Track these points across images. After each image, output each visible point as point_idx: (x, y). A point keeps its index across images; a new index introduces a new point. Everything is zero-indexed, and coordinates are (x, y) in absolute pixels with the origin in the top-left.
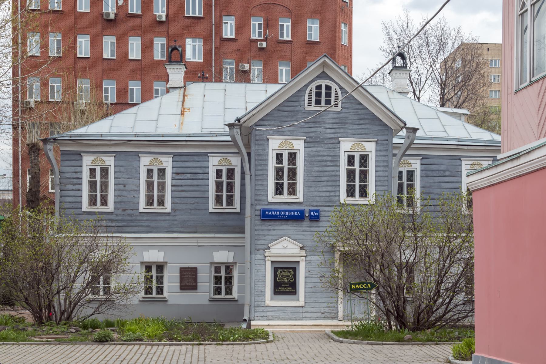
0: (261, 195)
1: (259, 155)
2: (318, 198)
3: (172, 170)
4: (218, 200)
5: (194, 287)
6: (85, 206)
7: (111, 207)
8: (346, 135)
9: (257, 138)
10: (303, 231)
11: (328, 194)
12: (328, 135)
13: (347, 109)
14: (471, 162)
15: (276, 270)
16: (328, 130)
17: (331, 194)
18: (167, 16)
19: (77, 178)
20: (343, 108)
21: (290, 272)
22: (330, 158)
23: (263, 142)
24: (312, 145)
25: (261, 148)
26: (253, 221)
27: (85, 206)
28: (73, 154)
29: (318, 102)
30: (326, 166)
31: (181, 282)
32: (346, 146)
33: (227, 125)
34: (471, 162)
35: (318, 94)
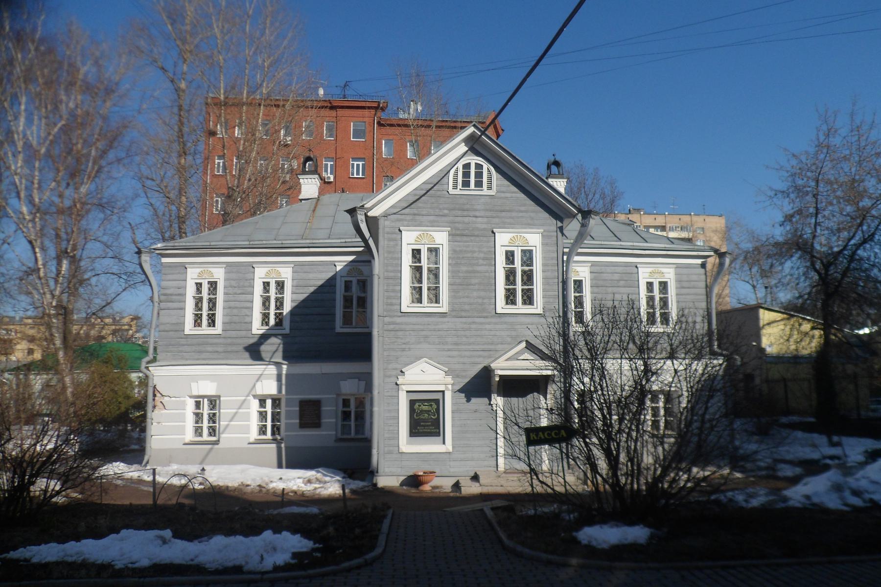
0: (391, 304)
1: (389, 252)
2: (467, 307)
5: (317, 425)
6: (189, 327)
7: (218, 329)
8: (504, 226)
9: (387, 230)
10: (449, 350)
11: (480, 301)
12: (479, 226)
13: (503, 192)
14: (650, 270)
15: (412, 403)
16: (479, 219)
17: (485, 301)
18: (335, 178)
19: (179, 295)
20: (498, 192)
21: (431, 405)
22: (482, 255)
23: (395, 236)
24: (458, 238)
25: (392, 243)
26: (381, 338)
27: (189, 327)
28: (176, 266)
29: (466, 184)
30: (477, 265)
31: (300, 419)
32: (503, 239)
33: (346, 211)
34: (650, 270)
35: (466, 174)
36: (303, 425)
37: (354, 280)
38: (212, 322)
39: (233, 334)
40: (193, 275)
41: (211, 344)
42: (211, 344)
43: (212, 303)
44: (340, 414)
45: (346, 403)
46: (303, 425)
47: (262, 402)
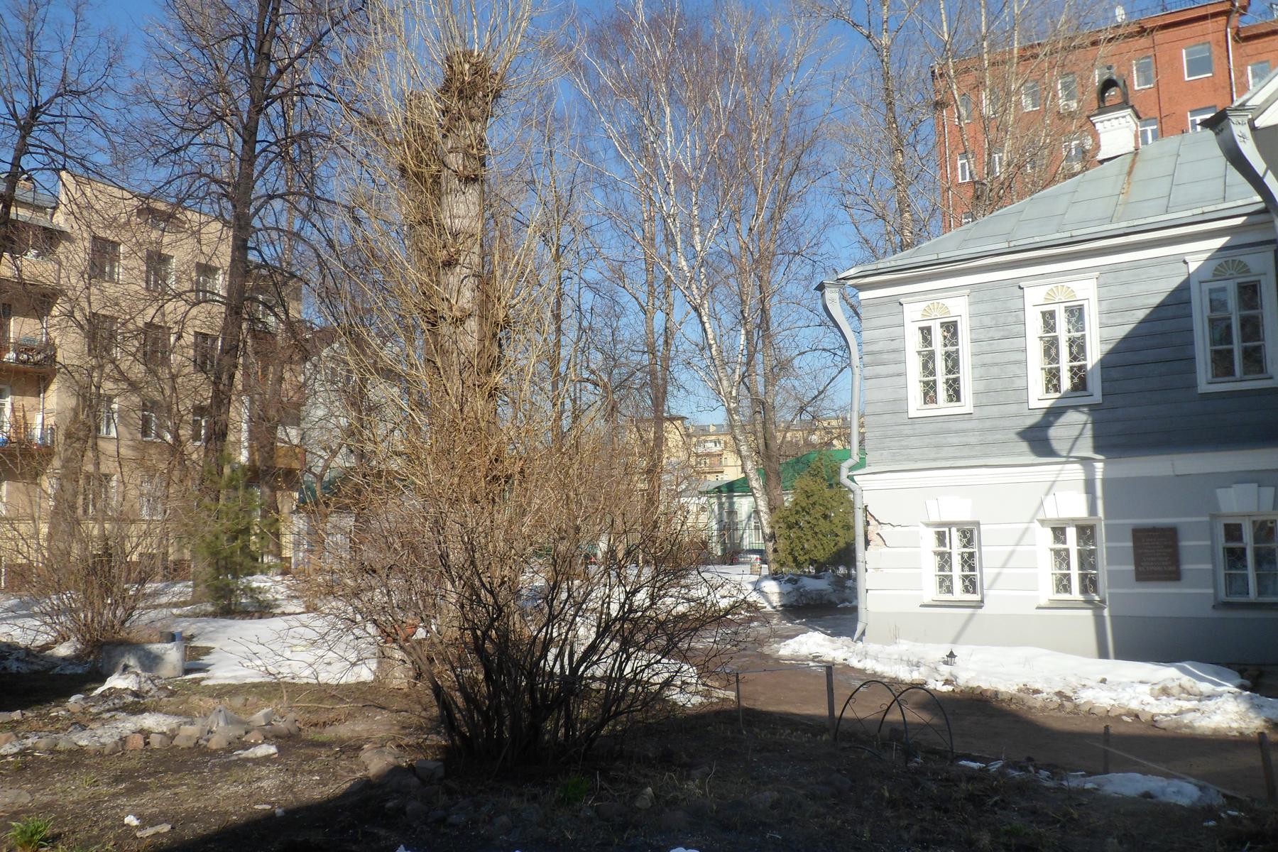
3: (1100, 305)
4: (1222, 363)
5: (1173, 574)
6: (915, 405)
27: (915, 405)
28: (884, 303)
36: (1143, 575)
37: (1231, 286)
38: (955, 393)
39: (994, 411)
40: (914, 314)
41: (956, 432)
42: (956, 432)
43: (953, 362)
44: (1220, 554)
45: (1233, 532)
46: (1143, 575)
47: (1059, 532)
